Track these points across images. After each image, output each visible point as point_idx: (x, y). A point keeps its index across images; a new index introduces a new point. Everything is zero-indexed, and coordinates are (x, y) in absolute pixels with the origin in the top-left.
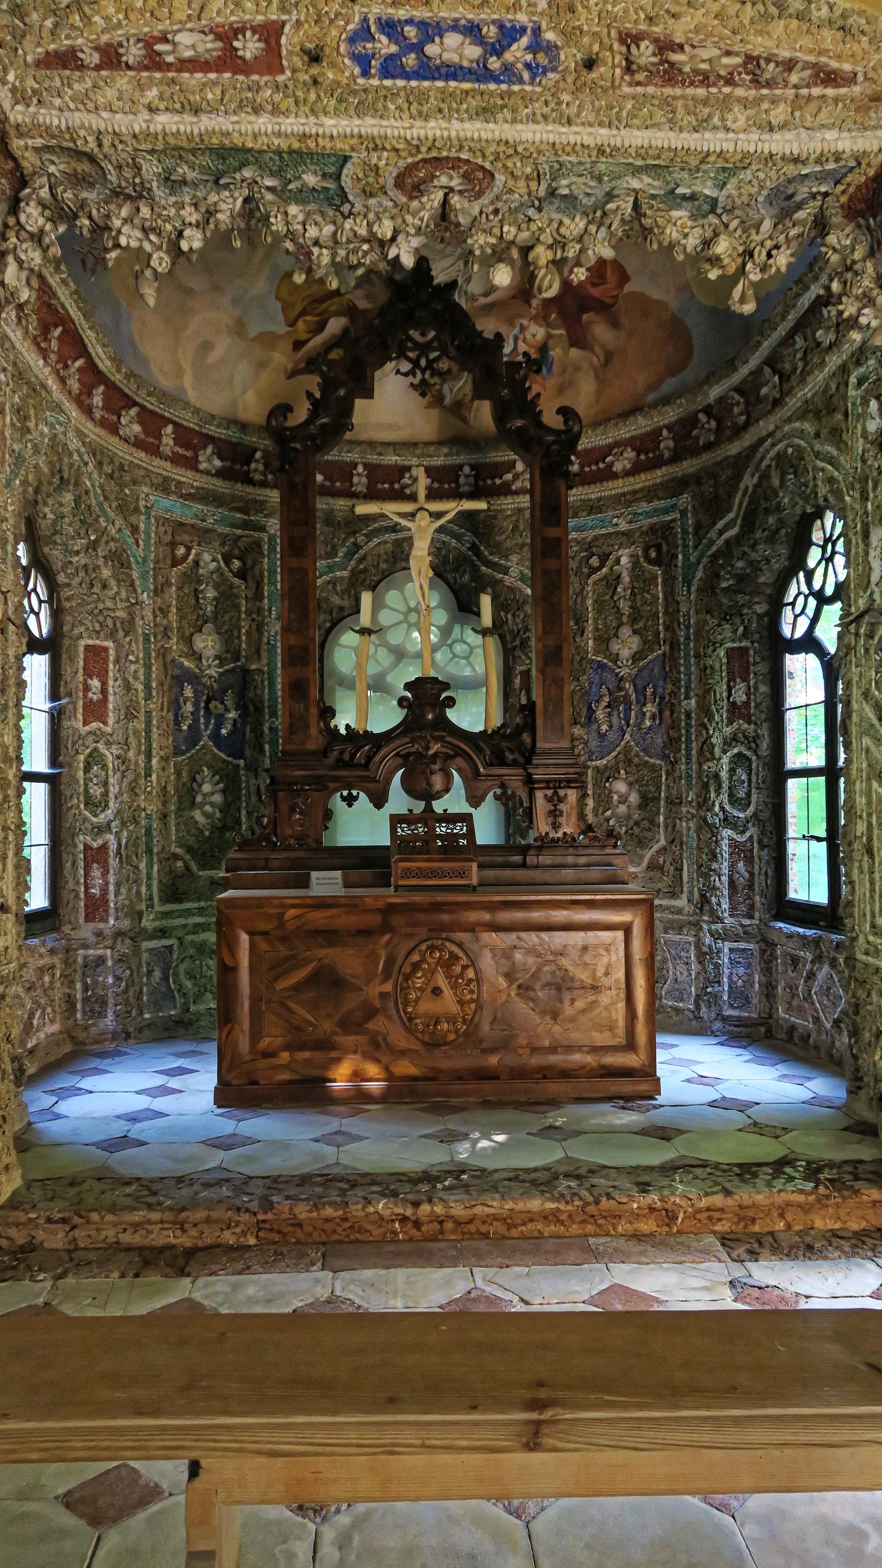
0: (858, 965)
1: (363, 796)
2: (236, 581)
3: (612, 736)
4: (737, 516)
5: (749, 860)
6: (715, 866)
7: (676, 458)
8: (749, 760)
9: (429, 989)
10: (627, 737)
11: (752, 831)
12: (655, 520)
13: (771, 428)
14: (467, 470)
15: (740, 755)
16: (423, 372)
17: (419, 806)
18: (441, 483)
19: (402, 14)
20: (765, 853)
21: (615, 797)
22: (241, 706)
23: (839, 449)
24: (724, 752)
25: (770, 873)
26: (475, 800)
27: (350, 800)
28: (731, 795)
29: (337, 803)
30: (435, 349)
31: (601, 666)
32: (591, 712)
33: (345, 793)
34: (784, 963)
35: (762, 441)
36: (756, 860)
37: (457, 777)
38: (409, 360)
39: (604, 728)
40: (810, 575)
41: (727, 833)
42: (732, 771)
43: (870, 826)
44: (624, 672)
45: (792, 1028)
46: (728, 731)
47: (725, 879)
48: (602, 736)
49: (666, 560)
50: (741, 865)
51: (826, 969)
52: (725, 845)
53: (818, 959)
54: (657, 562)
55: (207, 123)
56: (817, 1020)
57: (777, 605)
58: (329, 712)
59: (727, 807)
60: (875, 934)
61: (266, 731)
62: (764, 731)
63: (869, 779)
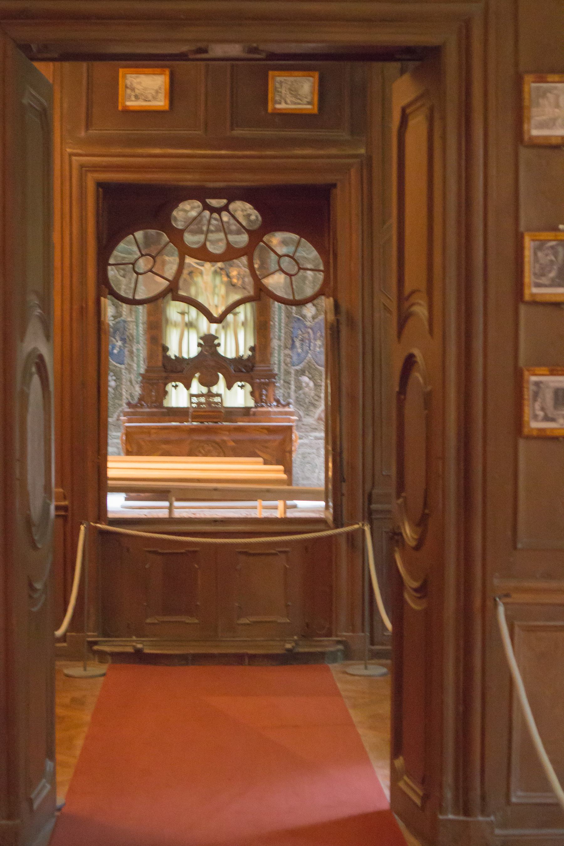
1: (181, 385)
2: (121, 278)
3: (303, 355)
10: (310, 355)
17: (204, 390)
21: (304, 385)
22: (123, 340)
26: (229, 386)
27: (176, 386)
29: (169, 387)
31: (299, 319)
32: (293, 342)
33: (174, 384)
37: (221, 376)
39: (300, 350)
44: (308, 324)
48: (299, 355)
58: (165, 349)
61: (135, 350)
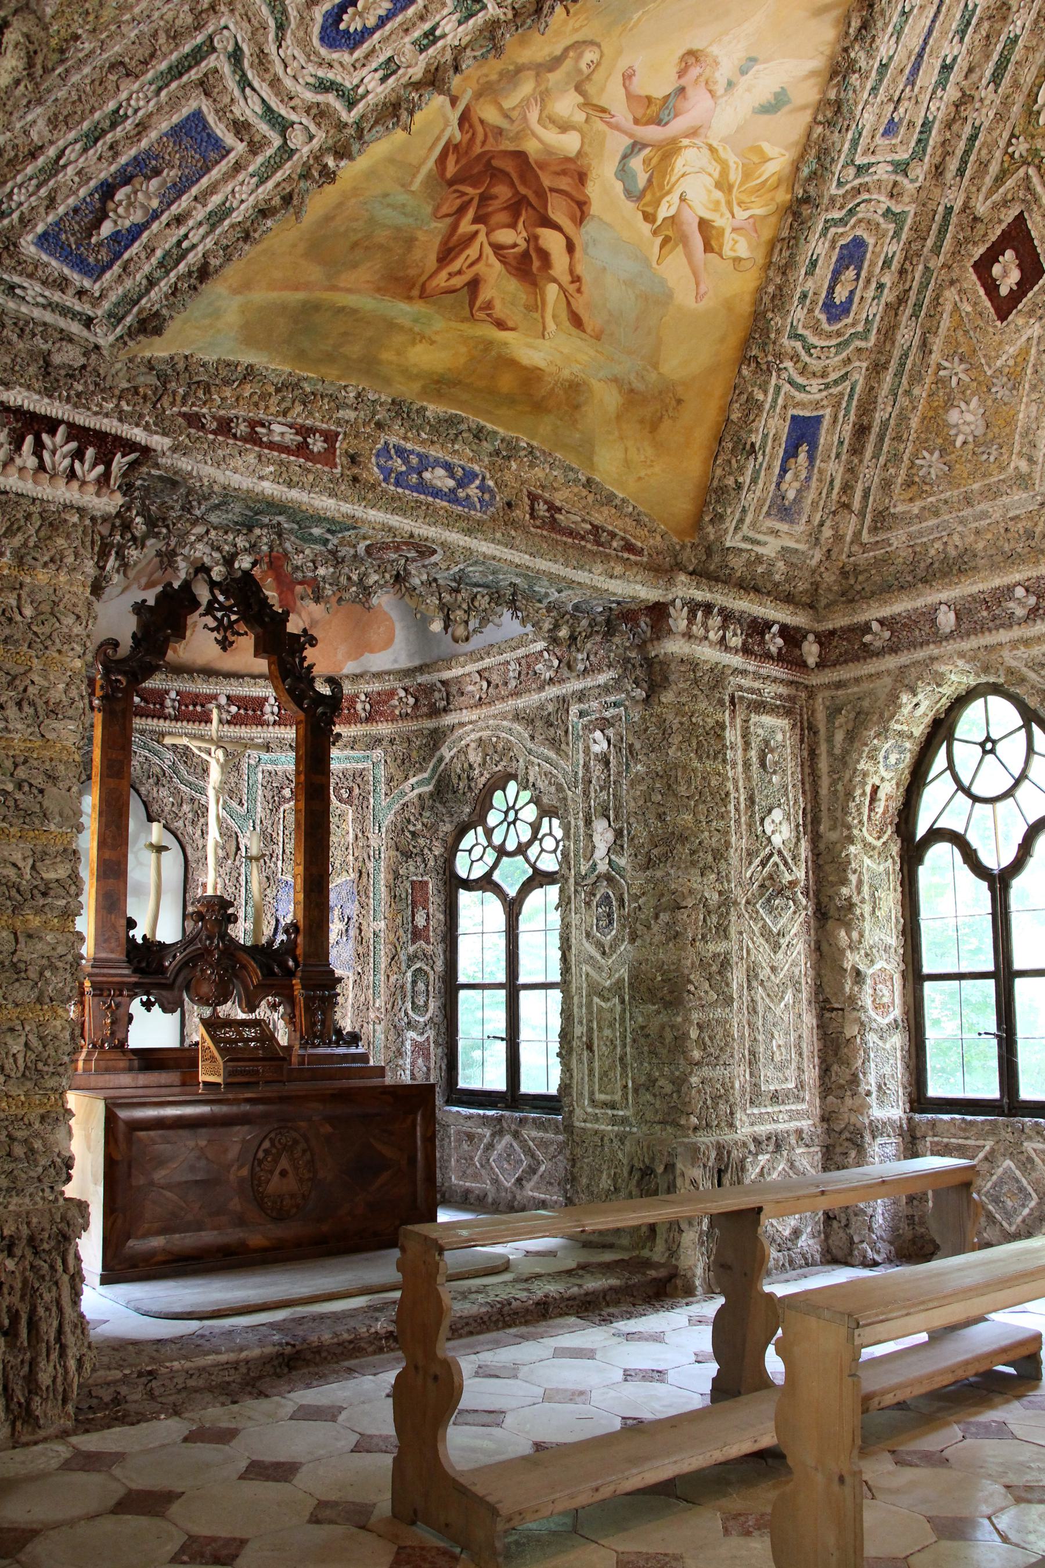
0: (575, 1131)
4: (431, 778)
5: (427, 1057)
6: (401, 1062)
7: (369, 719)
8: (426, 973)
9: (277, 1172)
11: (431, 1033)
12: (349, 766)
13: (474, 717)
14: (173, 695)
15: (420, 969)
16: (225, 632)
18: (147, 702)
19: (409, 446)
20: (440, 1050)
23: (557, 754)
24: (409, 967)
25: (444, 1067)
28: (413, 1003)
29: (136, 1007)
30: (235, 613)
33: (145, 998)
34: (459, 1141)
35: (462, 725)
36: (432, 1056)
38: (215, 618)
40: (489, 833)
41: (411, 1034)
42: (414, 983)
43: (590, 1030)
45: (467, 1192)
46: (411, 949)
47: (408, 1072)
49: (356, 802)
50: (420, 1061)
51: (508, 1138)
52: (408, 1045)
53: (499, 1133)
54: (349, 802)
55: (294, 494)
56: (496, 1181)
57: (452, 850)
59: (410, 1012)
60: (595, 1107)
62: (440, 949)
63: (589, 995)
